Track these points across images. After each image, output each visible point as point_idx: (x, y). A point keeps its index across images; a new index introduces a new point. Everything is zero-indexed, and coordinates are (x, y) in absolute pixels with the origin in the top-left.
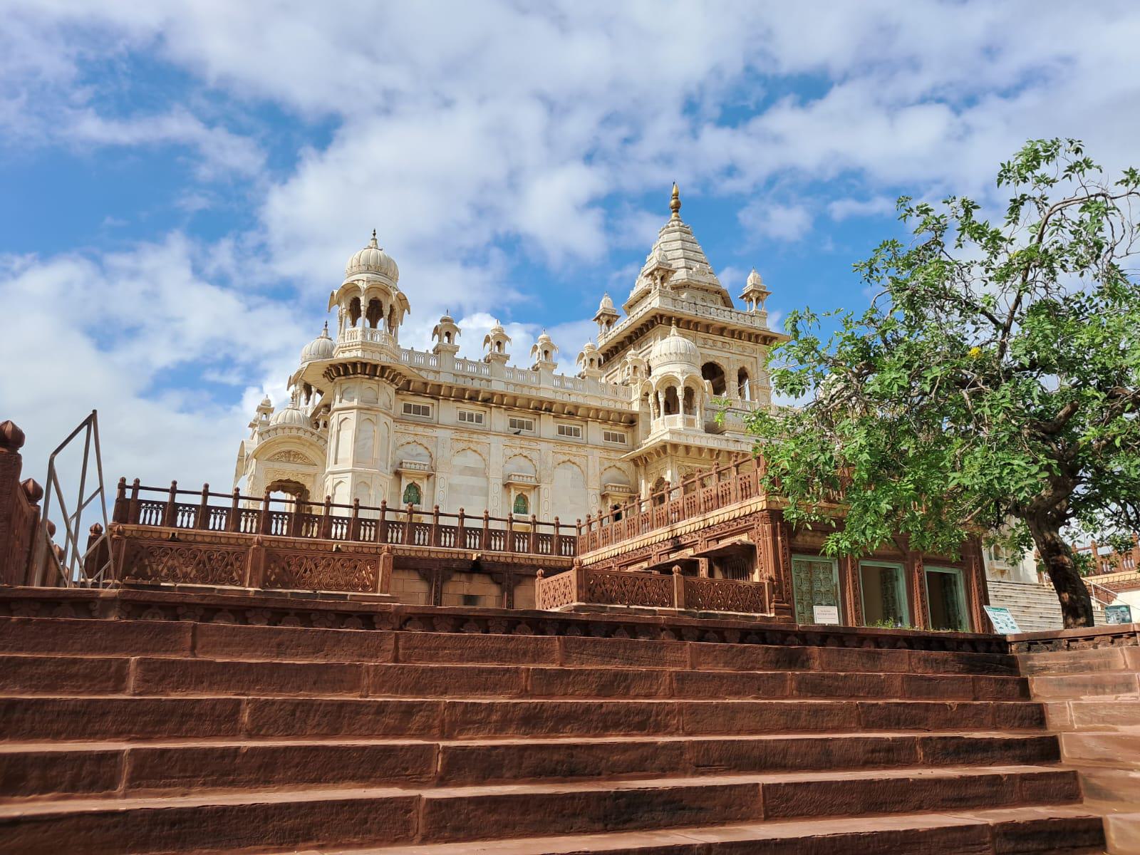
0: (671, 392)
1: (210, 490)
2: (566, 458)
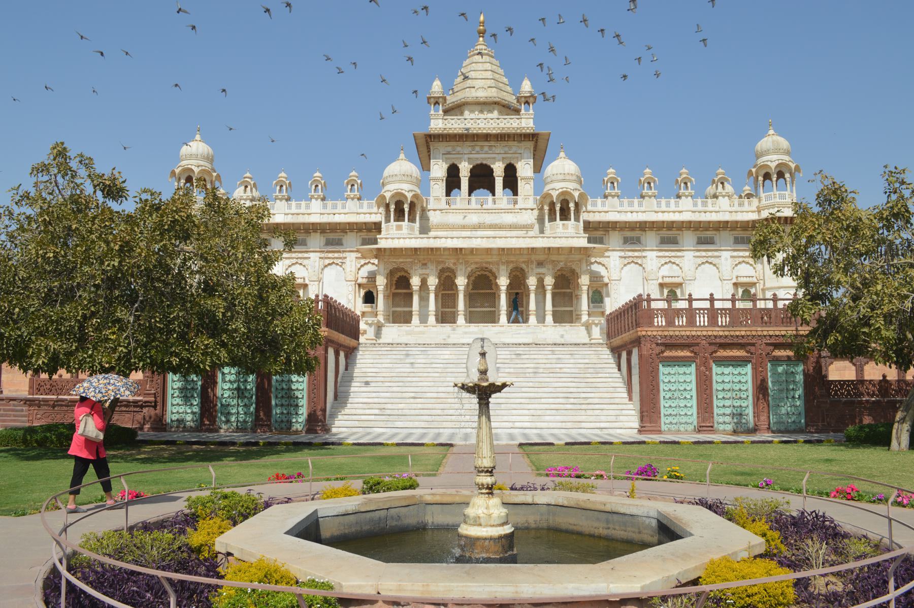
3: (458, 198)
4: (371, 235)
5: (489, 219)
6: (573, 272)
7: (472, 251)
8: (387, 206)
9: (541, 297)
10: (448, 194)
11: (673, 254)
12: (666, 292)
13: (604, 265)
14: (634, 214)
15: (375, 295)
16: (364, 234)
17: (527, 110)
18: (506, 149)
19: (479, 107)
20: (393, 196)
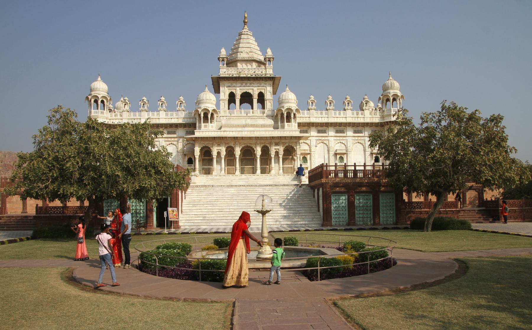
0: (206, 115)
2: (170, 143)
3: (235, 111)
4: (191, 129)
5: (249, 122)
6: (293, 148)
7: (242, 138)
8: (200, 115)
9: (277, 160)
10: (229, 109)
11: (341, 138)
12: (338, 156)
14: (323, 119)
15: (193, 159)
16: (187, 129)
17: (269, 65)
18: (259, 85)
20: (202, 110)
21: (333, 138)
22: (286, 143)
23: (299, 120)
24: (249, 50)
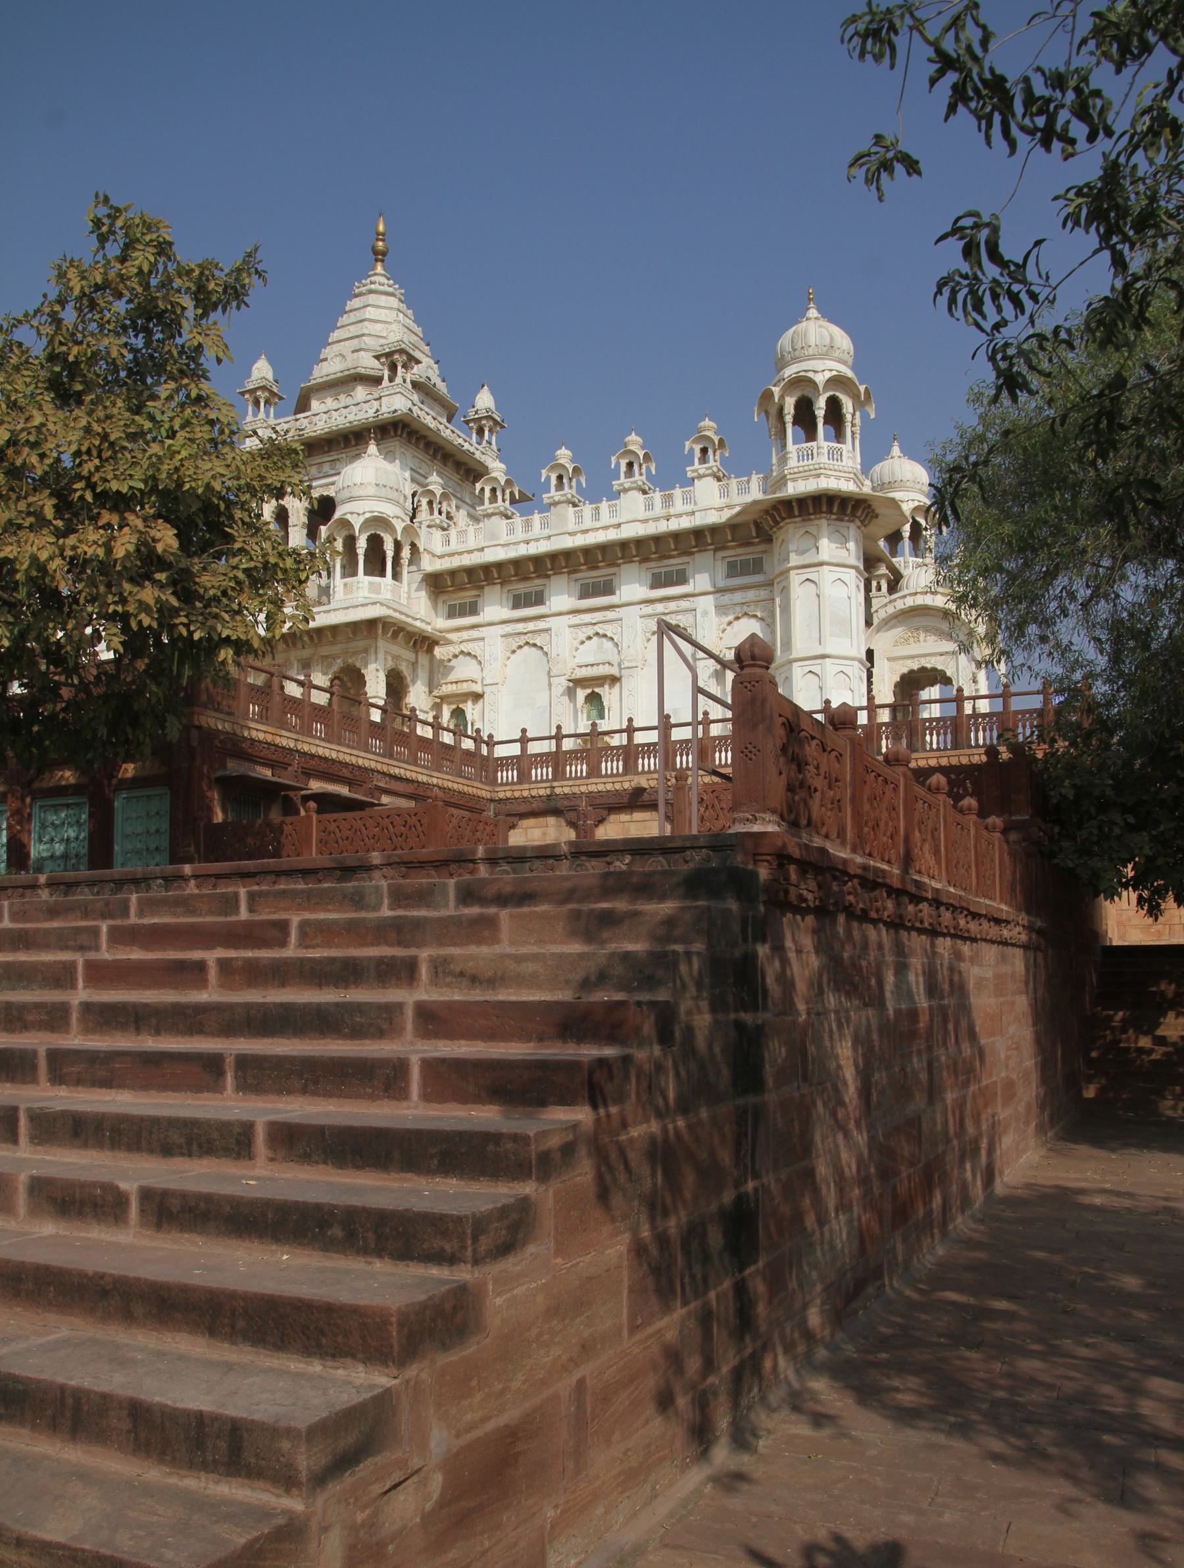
1: (636, 724)
13: (476, 657)
19: (333, 391)
21: (567, 617)
22: (334, 657)
23: (429, 565)
24: (355, 343)
